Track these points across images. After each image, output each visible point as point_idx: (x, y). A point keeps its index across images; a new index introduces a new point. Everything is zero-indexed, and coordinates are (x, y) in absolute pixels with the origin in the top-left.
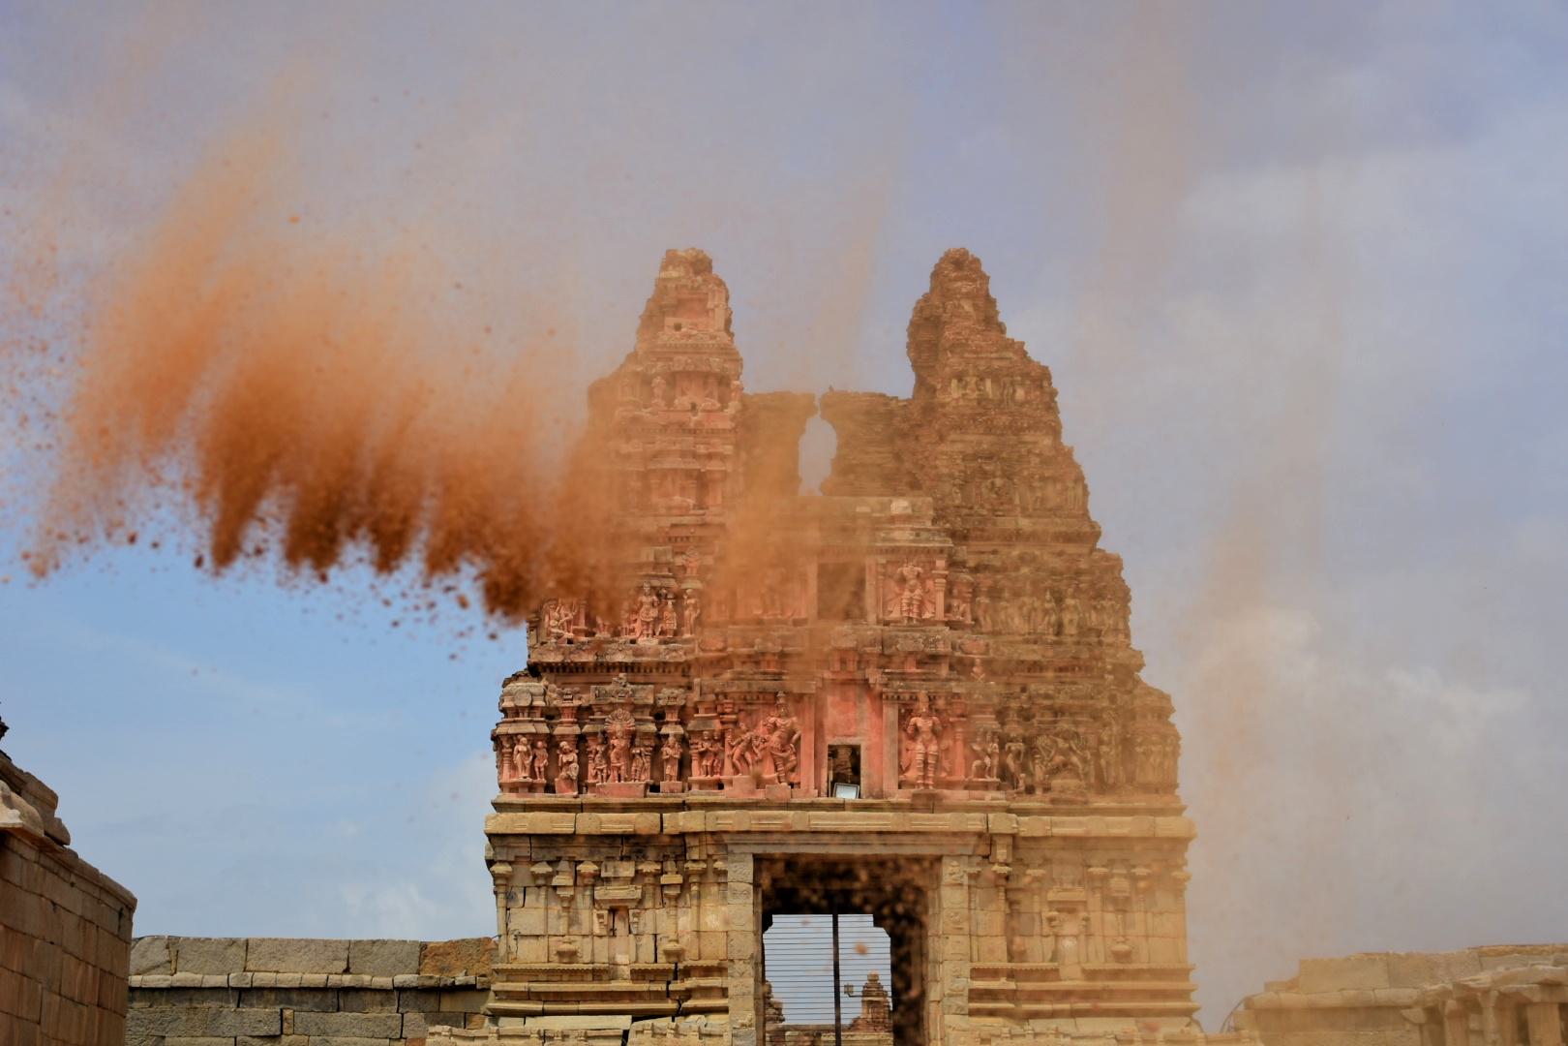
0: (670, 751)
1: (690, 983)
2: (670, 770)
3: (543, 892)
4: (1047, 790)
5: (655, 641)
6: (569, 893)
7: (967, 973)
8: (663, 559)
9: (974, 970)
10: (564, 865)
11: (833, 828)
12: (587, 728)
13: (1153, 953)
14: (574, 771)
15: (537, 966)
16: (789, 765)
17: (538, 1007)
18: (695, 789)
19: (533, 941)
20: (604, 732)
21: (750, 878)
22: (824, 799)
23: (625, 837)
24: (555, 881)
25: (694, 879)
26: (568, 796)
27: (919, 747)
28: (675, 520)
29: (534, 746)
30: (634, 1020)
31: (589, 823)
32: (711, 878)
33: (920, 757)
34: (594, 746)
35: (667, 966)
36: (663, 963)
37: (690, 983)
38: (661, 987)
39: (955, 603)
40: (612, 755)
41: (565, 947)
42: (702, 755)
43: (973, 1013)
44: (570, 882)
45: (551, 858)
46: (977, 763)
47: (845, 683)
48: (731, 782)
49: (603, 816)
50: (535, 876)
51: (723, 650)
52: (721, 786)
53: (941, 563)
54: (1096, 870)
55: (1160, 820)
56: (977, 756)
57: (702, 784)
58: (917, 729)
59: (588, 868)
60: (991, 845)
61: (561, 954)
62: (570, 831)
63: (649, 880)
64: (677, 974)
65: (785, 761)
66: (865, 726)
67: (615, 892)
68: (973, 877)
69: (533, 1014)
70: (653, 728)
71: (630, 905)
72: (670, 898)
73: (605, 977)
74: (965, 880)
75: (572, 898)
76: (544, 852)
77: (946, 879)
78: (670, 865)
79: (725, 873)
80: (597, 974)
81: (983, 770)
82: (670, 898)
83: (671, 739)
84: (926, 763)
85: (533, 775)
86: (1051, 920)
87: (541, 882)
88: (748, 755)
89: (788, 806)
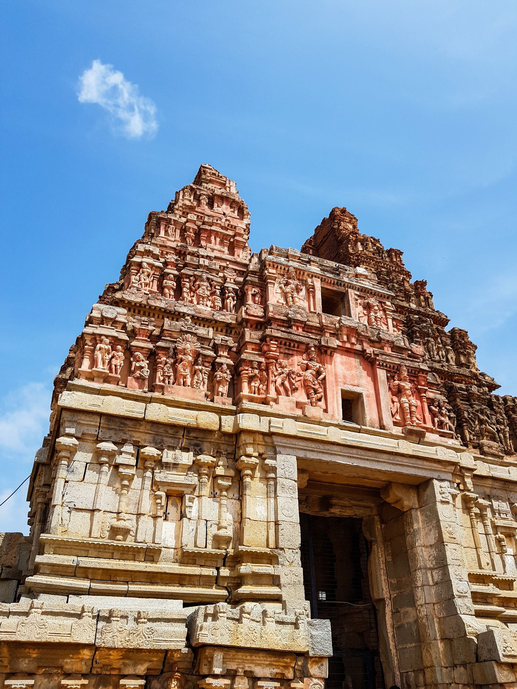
1: (245, 568)
2: (224, 389)
7: (466, 578)
8: (213, 267)
10: (129, 448)
17: (85, 584)
20: (175, 349)
23: (187, 429)
24: (120, 459)
28: (219, 255)
30: (185, 605)
31: (157, 412)
33: (407, 405)
37: (245, 568)
38: (211, 572)
40: (180, 367)
41: (121, 524)
42: (251, 379)
43: (479, 614)
44: (133, 461)
45: (118, 440)
48: (276, 401)
50: (99, 453)
59: (150, 451)
60: (462, 477)
65: (316, 392)
69: (78, 592)
72: (222, 488)
76: (112, 432)
77: (439, 497)
79: (274, 469)
87: (104, 459)
88: (287, 383)
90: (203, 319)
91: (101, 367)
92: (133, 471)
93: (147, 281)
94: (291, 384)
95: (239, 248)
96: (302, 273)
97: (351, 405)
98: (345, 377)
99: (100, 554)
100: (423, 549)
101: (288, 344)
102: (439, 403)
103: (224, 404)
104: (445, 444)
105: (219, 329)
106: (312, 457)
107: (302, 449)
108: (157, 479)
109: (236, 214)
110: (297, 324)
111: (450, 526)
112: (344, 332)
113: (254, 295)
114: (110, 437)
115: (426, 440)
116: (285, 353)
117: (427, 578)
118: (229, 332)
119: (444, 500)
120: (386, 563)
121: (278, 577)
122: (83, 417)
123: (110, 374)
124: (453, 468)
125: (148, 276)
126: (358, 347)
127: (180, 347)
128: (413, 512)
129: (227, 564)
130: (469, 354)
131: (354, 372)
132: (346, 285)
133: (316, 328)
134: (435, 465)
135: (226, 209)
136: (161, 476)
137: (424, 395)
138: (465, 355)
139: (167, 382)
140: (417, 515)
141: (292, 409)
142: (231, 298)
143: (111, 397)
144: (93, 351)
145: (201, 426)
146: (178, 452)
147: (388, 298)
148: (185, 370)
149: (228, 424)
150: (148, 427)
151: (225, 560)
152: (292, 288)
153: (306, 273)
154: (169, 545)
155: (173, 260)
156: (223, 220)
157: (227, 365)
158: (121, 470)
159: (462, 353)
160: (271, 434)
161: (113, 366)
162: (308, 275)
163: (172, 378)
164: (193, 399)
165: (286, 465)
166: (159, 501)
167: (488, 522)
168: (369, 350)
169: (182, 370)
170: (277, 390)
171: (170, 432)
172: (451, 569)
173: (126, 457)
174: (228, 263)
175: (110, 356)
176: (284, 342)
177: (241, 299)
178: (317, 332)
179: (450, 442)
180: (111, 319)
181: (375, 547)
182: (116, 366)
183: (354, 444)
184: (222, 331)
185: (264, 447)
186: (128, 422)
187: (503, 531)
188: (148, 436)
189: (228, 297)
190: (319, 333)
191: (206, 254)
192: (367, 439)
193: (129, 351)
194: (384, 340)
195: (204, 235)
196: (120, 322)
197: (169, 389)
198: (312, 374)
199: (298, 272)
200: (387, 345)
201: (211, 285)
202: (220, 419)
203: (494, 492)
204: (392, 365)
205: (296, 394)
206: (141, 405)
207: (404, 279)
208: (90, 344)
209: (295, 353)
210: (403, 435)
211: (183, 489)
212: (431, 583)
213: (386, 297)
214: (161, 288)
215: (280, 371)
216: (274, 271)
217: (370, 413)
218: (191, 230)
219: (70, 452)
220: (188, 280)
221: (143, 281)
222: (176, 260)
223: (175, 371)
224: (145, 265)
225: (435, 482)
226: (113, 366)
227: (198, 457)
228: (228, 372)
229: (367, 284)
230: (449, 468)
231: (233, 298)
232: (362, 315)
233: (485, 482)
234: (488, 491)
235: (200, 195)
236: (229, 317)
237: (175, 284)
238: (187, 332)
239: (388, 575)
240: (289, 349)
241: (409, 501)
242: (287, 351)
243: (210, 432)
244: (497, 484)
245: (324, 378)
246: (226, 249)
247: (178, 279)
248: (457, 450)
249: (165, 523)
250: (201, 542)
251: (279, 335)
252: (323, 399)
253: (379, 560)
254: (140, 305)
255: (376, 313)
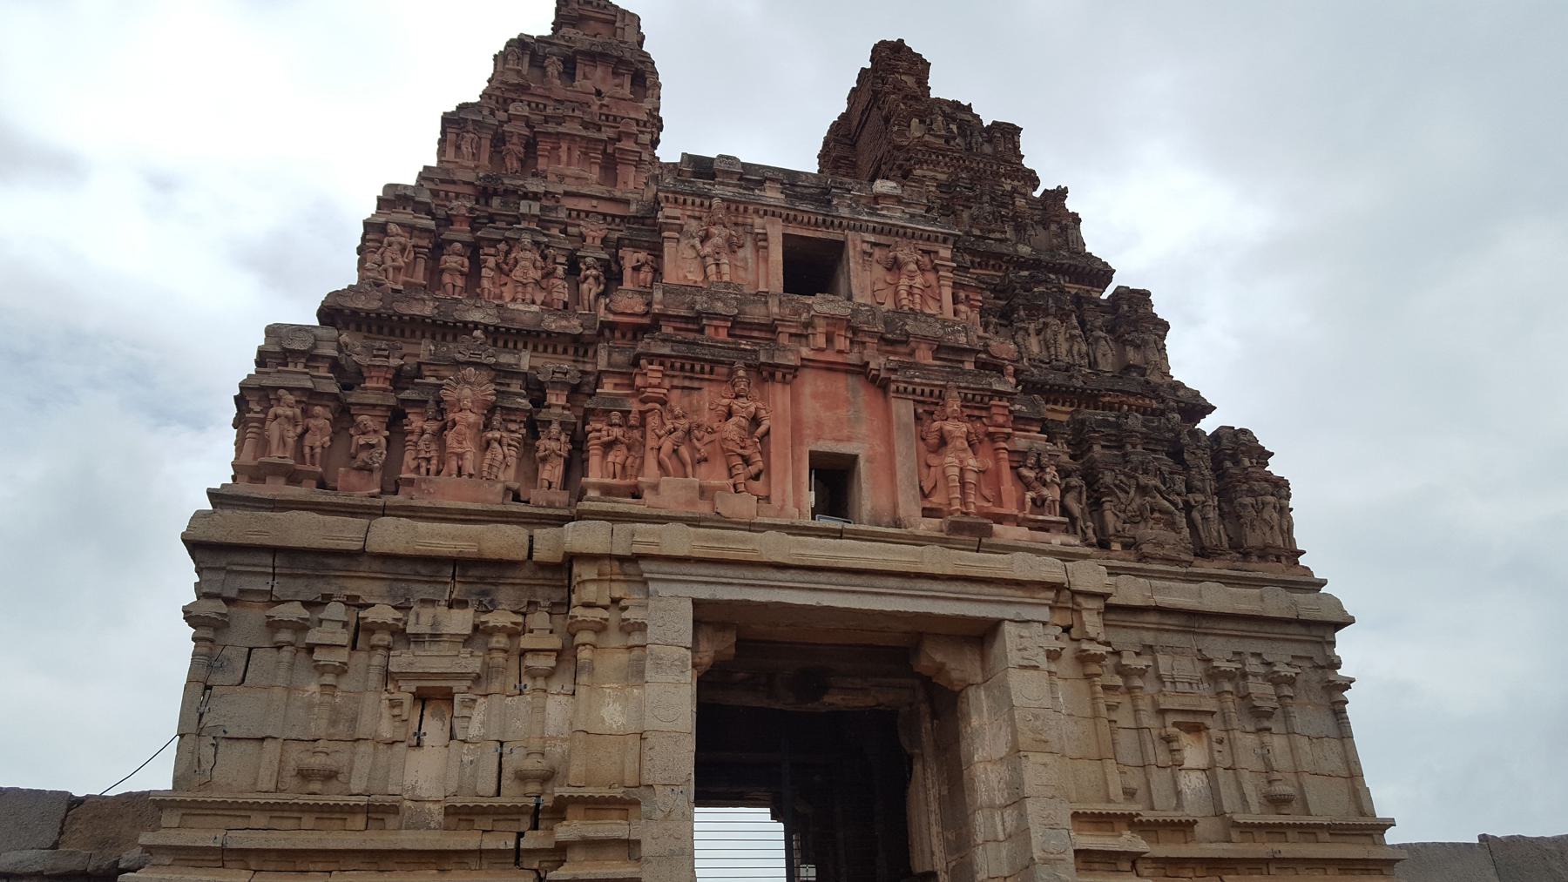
0: (553, 445)
2: (552, 472)
3: (286, 654)
4: (1125, 546)
5: (535, 308)
6: (342, 656)
7: (1066, 821)
9: (1075, 815)
10: (335, 610)
11: (831, 563)
12: (406, 394)
13: (1326, 806)
14: (379, 457)
15: (251, 798)
16: (753, 469)
18: (592, 493)
19: (251, 747)
20: (439, 401)
21: (688, 641)
22: (807, 521)
23: (460, 565)
24: (313, 637)
25: (582, 637)
26: (365, 490)
27: (950, 459)
28: (573, 189)
29: (306, 413)
31: (391, 535)
32: (614, 639)
33: (954, 472)
34: (415, 421)
35: (520, 802)
36: (513, 796)
39: (962, 308)
40: (450, 436)
41: (317, 762)
42: (608, 446)
44: (344, 637)
45: (311, 596)
46: (1029, 495)
47: (830, 367)
48: (655, 488)
49: (422, 526)
50: (274, 625)
51: (646, 314)
52: (636, 494)
53: (945, 253)
54: (1224, 666)
55: (1298, 596)
56: (1028, 486)
57: (607, 491)
58: (943, 441)
59: (382, 613)
60: (1077, 611)
61: (305, 775)
62: (356, 546)
63: (500, 641)
64: (536, 816)
65: (747, 461)
66: (863, 430)
67: (432, 661)
68: (1053, 656)
70: (524, 403)
71: (457, 686)
72: (533, 674)
73: (392, 821)
74: (1042, 660)
75: (341, 670)
76: (300, 584)
77: (1014, 658)
78: (539, 619)
79: (641, 627)
80: (378, 812)
81: (1039, 503)
82: (533, 674)
83: (555, 428)
84: (963, 484)
85: (299, 455)
86: (1168, 740)
88: (685, 452)
89: (752, 527)
90: (519, 331)
91: (276, 455)
92: (342, 656)
93: (401, 262)
94: (694, 449)
95: (625, 163)
96: (741, 208)
97: (834, 481)
98: (819, 424)
99: (275, 823)
100: (989, 767)
101: (688, 367)
102: (1038, 460)
103: (551, 505)
104: (1045, 547)
105: (560, 349)
106: (727, 597)
107: (706, 583)
108: (391, 669)
109: (626, 91)
110: (715, 323)
111: (1036, 717)
112: (820, 330)
113: (636, 269)
114: (297, 593)
115: (994, 540)
116: (683, 388)
117: (994, 826)
118: (581, 352)
119: (1025, 663)
120: (941, 800)
121: (638, 842)
122: (237, 558)
123: (299, 467)
124: (1052, 594)
125: (403, 249)
126: (853, 358)
127: (448, 395)
128: (971, 692)
129: (541, 826)
130: (1145, 342)
131: (842, 413)
132: (845, 223)
133: (761, 327)
134: (1009, 592)
135: (604, 80)
136: (402, 660)
137: (1004, 445)
138: (1137, 347)
139: (423, 470)
140: (978, 698)
141: (691, 503)
142: (591, 280)
143: (295, 513)
144: (263, 422)
145: (488, 555)
146: (442, 610)
147: (945, 241)
148: (460, 442)
149: (548, 543)
150: (376, 565)
151: (536, 816)
152: (717, 246)
153: (751, 208)
154: (424, 794)
155: (463, 211)
156: (595, 108)
157: (561, 424)
158: (318, 655)
159: (1132, 343)
160: (637, 558)
161: (307, 450)
162: (756, 212)
163: (434, 461)
164: (475, 501)
165: (669, 615)
166: (396, 711)
167: (1145, 704)
168: (877, 362)
169: (455, 445)
170: (660, 464)
171: (423, 571)
172: (1031, 806)
173: (331, 628)
174: (594, 202)
175: (299, 430)
176: (678, 365)
177: (611, 276)
178: (763, 335)
179: (1057, 540)
180: (303, 352)
181: (918, 767)
182: (312, 448)
183: (820, 562)
184: (565, 351)
185: (624, 586)
186: (332, 561)
187: (1180, 718)
188: (378, 583)
189: (586, 278)
190: (769, 336)
191: (541, 190)
192: (852, 550)
193: (344, 415)
194: (915, 336)
195: (544, 146)
196: (324, 357)
197: (424, 486)
198: (740, 427)
199: (733, 207)
200: (923, 346)
201: (544, 258)
202: (531, 538)
203: (1166, 639)
204: (927, 390)
205: (703, 469)
206: (360, 522)
207: (1014, 190)
208: (258, 409)
209: (705, 384)
210: (943, 535)
211: (450, 684)
212: (1001, 836)
213: (941, 237)
214: (435, 272)
215: (669, 426)
216: (677, 212)
217: (868, 495)
218: (515, 140)
219: (216, 629)
220: (492, 251)
221: (389, 262)
222: (471, 210)
223: (442, 445)
224: (393, 228)
225: (1008, 628)
226: (307, 450)
227: (484, 618)
228: (563, 438)
229: (895, 216)
230: (1042, 595)
231: (596, 278)
232: (880, 285)
233: (1140, 618)
234: (1149, 638)
235: (545, 57)
236: (576, 322)
237: (466, 262)
238: (469, 364)
239: (944, 827)
240: (691, 378)
241: (959, 666)
242: (687, 383)
243: (513, 564)
244: (1171, 621)
245: (768, 432)
246: (594, 173)
247: (474, 251)
248: (1066, 556)
249: (415, 755)
250: (487, 784)
251: (666, 350)
252: (762, 477)
253: (926, 793)
254: (379, 315)
255: (911, 278)
